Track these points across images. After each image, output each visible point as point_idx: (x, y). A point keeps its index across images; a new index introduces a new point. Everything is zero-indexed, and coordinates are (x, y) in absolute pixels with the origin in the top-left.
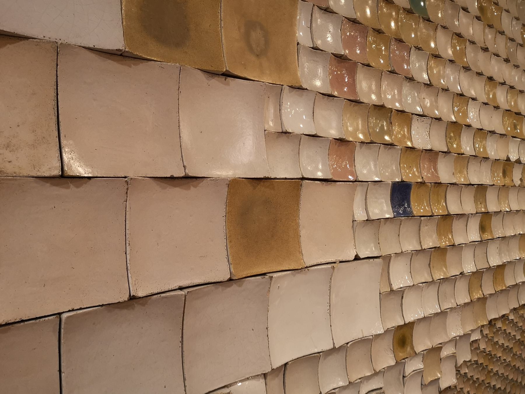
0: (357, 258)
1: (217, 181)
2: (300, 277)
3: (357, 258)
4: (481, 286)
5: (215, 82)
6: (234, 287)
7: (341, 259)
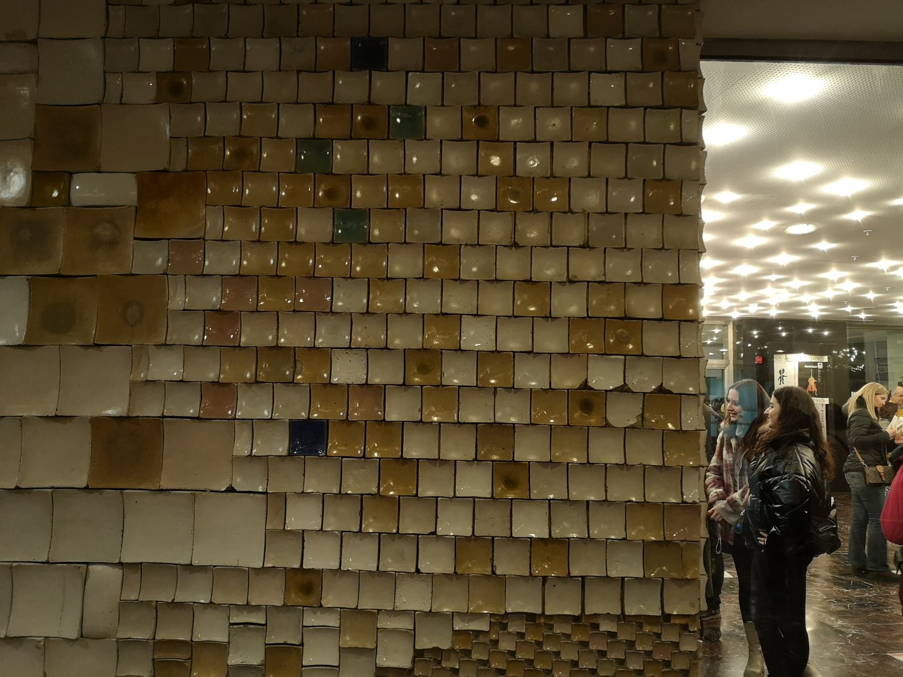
0: (231, 490)
1: (82, 418)
2: (160, 497)
3: (231, 490)
4: (492, 560)
5: (90, 351)
6: (96, 495)
7: (212, 489)
